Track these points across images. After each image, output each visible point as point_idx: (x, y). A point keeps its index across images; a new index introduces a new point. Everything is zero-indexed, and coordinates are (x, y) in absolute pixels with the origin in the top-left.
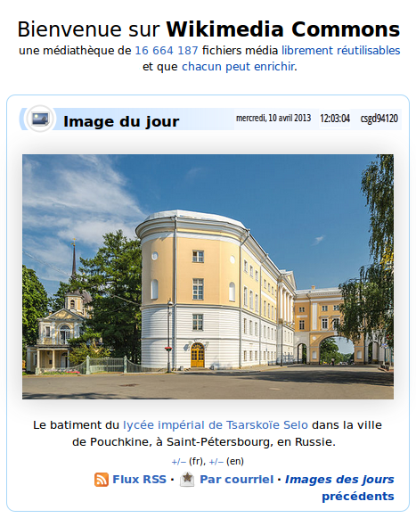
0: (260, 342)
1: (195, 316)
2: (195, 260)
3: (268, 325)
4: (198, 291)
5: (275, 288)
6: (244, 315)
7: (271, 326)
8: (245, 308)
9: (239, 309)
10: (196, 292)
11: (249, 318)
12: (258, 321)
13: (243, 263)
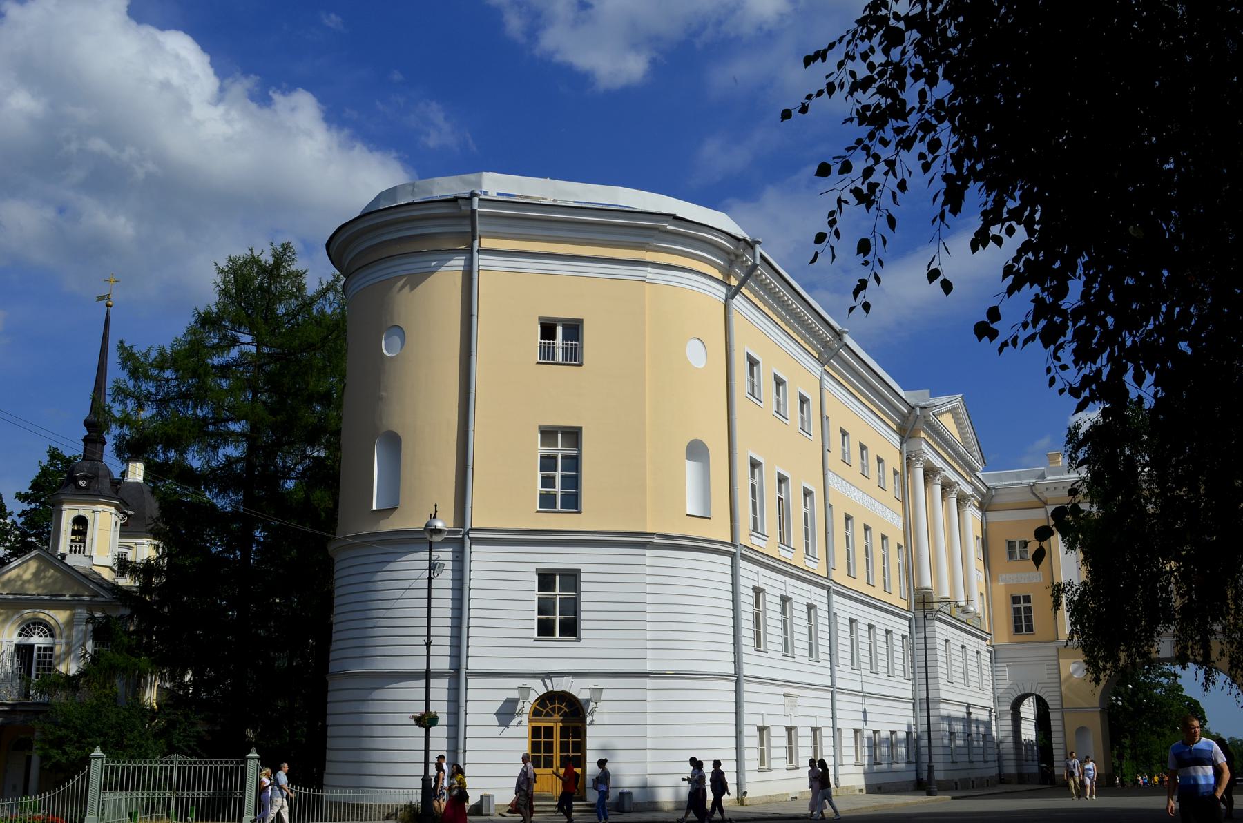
0: (833, 689)
2: (547, 355)
3: (865, 615)
4: (558, 475)
5: (893, 461)
6: (750, 574)
7: (883, 621)
8: (757, 543)
9: (734, 552)
10: (547, 482)
11: (774, 584)
12: (818, 596)
13: (741, 367)
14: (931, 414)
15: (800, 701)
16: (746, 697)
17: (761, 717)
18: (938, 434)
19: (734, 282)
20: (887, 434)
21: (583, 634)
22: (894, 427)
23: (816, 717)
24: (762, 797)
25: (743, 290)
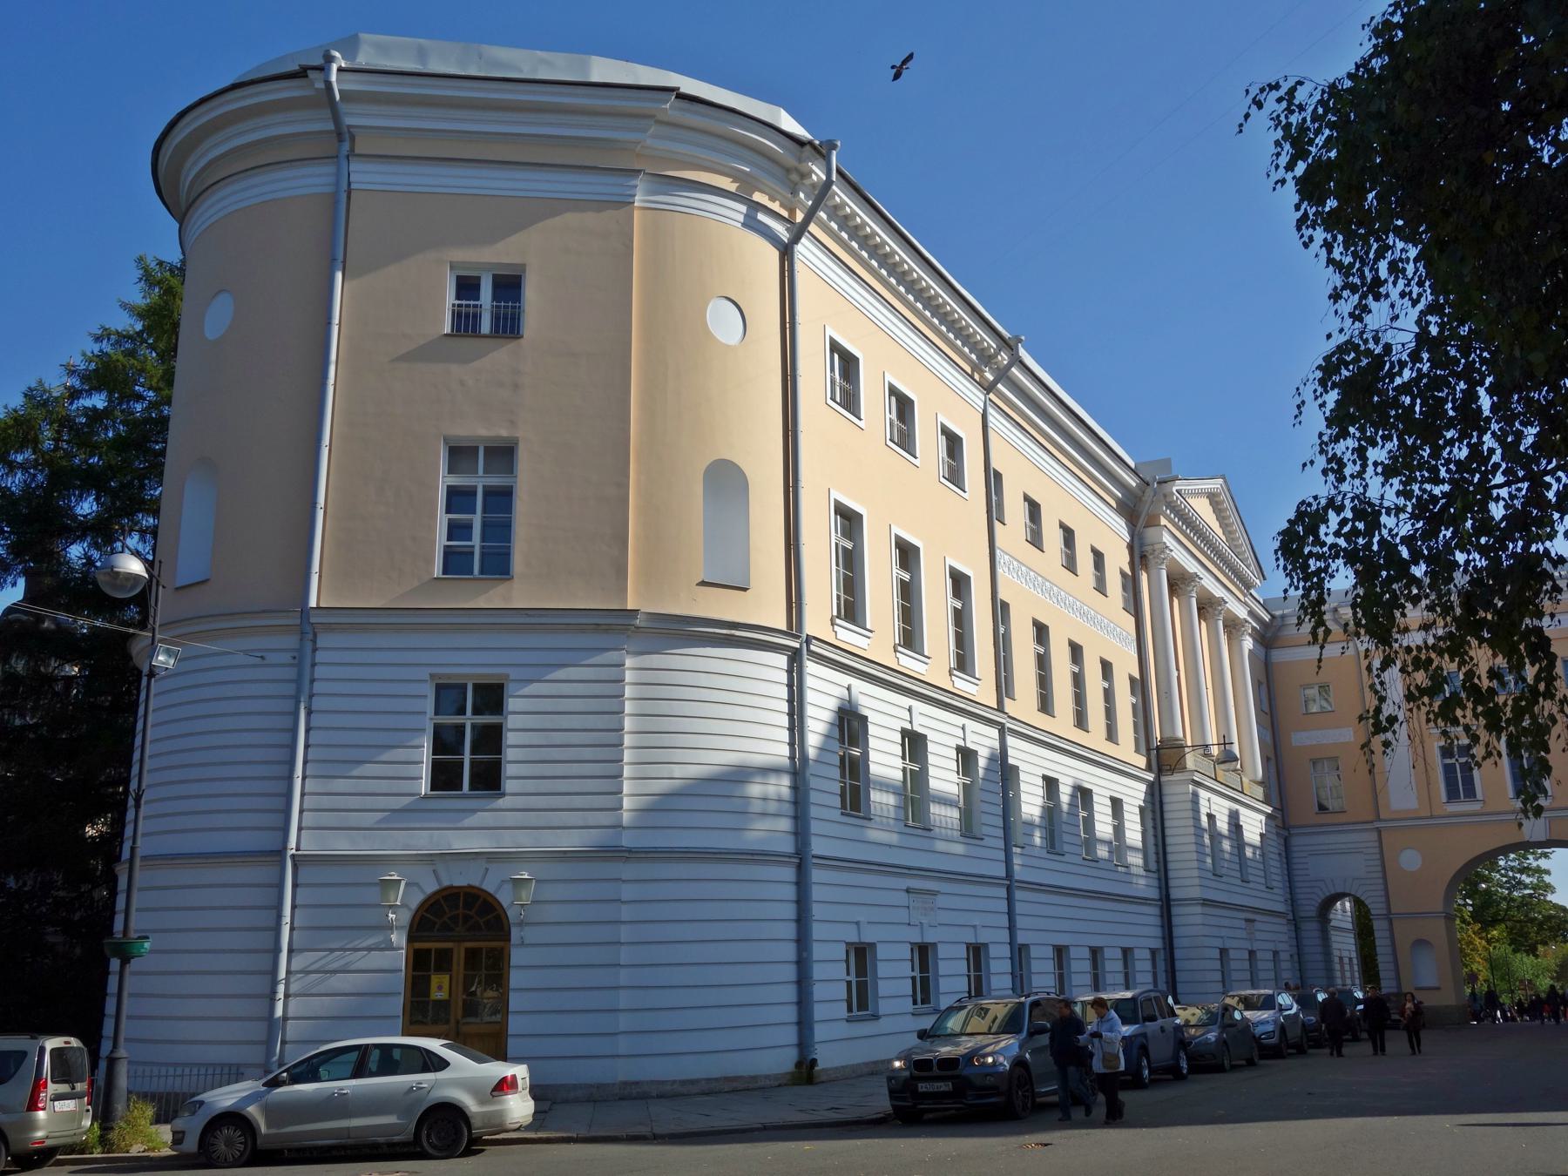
1: (448, 694)
4: (477, 520)
5: (1118, 560)
8: (847, 636)
10: (457, 530)
14: (1175, 492)
15: (941, 901)
16: (817, 893)
17: (855, 926)
18: (1188, 522)
19: (799, 217)
20: (1104, 514)
21: (509, 785)
22: (1114, 504)
23: (974, 927)
24: (858, 1065)
25: (813, 228)
